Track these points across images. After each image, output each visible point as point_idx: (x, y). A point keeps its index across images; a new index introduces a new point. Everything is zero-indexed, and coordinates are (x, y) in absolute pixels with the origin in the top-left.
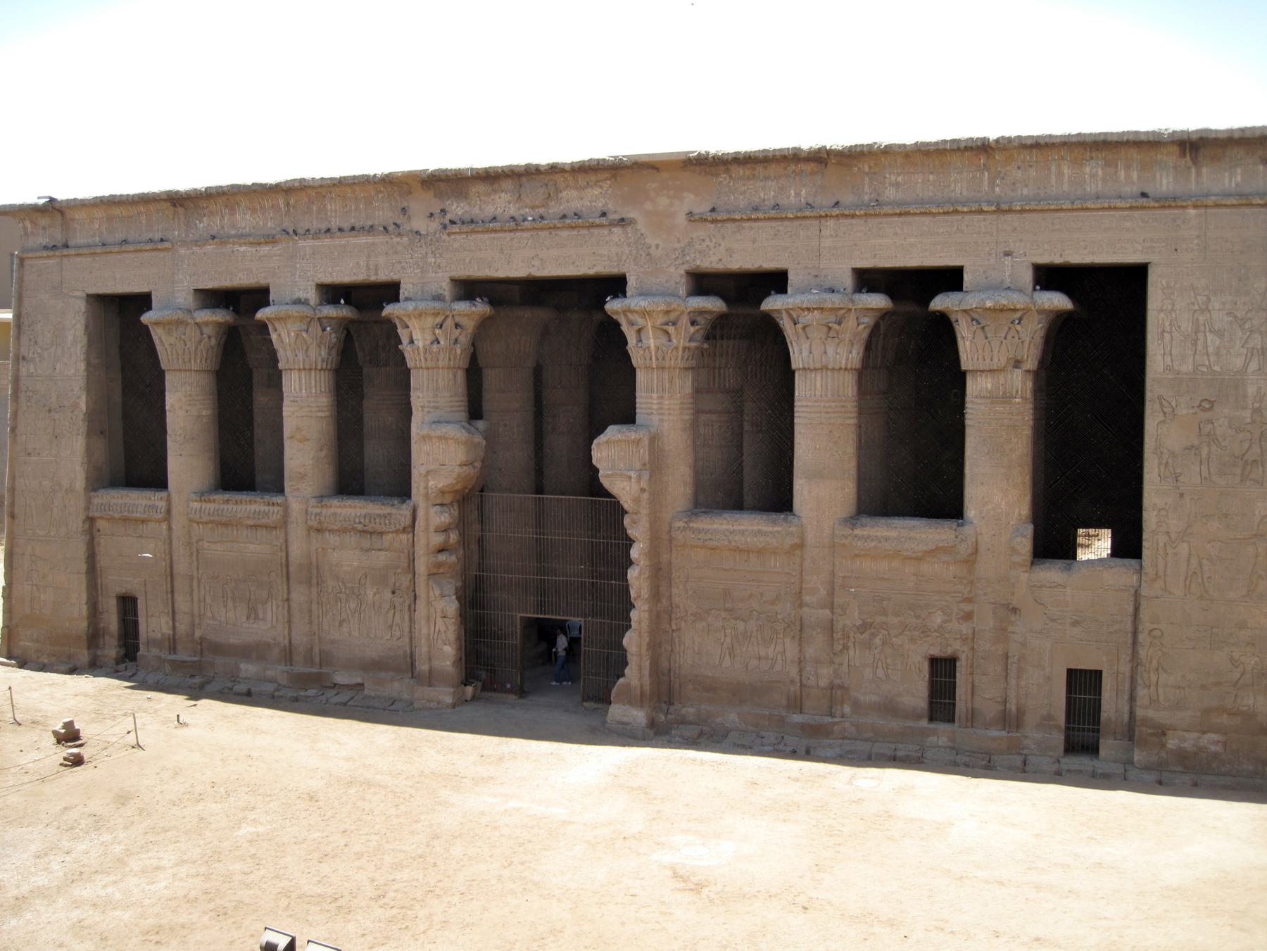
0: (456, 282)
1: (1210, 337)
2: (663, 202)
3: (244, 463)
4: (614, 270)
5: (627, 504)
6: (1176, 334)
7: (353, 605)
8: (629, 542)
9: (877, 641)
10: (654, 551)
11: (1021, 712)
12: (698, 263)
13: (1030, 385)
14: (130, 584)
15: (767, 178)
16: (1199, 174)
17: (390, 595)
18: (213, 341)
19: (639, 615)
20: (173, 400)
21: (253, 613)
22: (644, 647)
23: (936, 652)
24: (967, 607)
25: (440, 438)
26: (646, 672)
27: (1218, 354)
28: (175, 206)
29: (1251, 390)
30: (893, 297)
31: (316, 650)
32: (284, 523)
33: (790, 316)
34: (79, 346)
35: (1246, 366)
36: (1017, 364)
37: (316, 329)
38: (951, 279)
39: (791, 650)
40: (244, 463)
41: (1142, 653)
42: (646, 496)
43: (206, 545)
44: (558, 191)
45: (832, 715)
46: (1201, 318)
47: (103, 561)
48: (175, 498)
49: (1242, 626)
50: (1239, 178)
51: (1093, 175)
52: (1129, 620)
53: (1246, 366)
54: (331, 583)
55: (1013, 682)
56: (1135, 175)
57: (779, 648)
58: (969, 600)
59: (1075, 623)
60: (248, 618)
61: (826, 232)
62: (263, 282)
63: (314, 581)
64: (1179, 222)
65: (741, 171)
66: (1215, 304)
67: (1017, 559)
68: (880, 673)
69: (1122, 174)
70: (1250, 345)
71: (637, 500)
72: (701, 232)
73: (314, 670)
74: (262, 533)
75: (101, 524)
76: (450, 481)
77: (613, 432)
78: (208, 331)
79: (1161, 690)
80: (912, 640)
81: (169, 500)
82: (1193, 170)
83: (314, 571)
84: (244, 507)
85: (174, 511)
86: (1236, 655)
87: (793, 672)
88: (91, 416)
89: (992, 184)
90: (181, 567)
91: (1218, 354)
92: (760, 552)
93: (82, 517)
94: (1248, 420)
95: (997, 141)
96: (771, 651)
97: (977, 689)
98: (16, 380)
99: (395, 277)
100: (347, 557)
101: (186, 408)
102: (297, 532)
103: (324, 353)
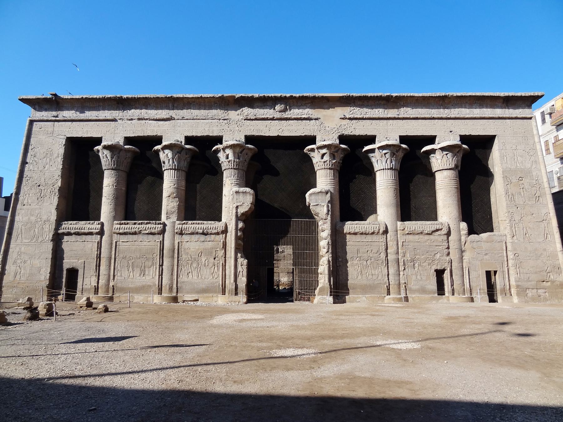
0: (246, 137)
9: (416, 265)
12: (343, 133)
21: (143, 273)
23: (439, 268)
25: (243, 192)
27: (522, 162)
28: (118, 103)
29: (534, 174)
32: (163, 232)
34: (60, 158)
43: (121, 243)
49: (545, 250)
59: (486, 254)
60: (140, 275)
61: (389, 124)
63: (176, 255)
66: (518, 147)
68: (419, 277)
73: (174, 295)
76: (247, 209)
78: (129, 155)
80: (429, 264)
83: (176, 252)
84: (143, 226)
86: (544, 261)
91: (522, 162)
96: (377, 271)
100: (192, 245)
103: (186, 163)
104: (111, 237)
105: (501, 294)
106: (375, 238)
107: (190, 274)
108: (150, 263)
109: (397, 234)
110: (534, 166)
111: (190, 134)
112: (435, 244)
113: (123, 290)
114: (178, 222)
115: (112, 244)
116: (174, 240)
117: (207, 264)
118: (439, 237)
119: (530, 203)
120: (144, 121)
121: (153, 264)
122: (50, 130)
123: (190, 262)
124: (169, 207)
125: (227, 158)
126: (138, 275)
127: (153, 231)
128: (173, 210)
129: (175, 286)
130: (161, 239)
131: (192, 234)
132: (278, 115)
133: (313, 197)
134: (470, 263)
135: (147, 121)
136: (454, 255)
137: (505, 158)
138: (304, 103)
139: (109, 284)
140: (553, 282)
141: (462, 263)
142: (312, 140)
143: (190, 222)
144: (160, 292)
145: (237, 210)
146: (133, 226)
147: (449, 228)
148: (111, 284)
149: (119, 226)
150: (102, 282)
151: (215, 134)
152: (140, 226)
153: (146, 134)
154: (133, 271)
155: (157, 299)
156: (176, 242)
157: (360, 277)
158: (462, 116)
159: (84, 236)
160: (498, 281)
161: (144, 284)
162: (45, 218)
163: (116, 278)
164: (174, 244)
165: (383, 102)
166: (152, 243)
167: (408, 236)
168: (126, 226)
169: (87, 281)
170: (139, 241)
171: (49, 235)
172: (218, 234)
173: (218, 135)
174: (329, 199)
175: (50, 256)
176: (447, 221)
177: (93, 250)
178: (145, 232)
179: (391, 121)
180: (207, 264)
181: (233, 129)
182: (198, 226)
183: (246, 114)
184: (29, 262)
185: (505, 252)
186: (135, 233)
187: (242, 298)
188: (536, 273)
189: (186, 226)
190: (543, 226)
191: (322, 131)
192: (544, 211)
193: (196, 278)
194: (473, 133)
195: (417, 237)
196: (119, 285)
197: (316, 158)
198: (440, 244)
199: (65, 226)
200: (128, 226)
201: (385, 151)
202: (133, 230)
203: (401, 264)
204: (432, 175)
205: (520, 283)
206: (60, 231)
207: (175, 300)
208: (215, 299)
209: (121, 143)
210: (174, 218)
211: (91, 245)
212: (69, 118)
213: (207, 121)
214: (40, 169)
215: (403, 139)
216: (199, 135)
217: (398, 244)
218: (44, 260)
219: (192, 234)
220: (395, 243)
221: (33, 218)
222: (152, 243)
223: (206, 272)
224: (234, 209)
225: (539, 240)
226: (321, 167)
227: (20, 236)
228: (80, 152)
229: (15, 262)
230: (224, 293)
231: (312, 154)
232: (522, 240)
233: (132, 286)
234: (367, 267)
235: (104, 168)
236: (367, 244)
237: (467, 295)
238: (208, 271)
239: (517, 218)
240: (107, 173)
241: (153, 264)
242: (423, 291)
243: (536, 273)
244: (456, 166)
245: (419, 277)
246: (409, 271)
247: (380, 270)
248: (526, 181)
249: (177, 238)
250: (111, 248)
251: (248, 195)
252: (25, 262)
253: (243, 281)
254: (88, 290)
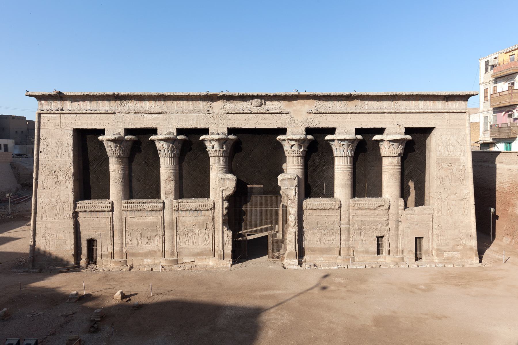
1: (451, 147)
9: (363, 233)
14: (92, 235)
21: (149, 241)
23: (379, 235)
25: (228, 179)
27: (453, 151)
29: (462, 161)
34: (70, 147)
49: (462, 222)
54: (181, 228)
59: (417, 224)
60: (147, 243)
62: (154, 127)
63: (175, 227)
66: (452, 138)
68: (364, 242)
72: (311, 116)
78: (129, 143)
80: (372, 232)
83: (175, 225)
84: (146, 204)
86: (461, 230)
91: (453, 151)
99: (207, 127)
100: (187, 219)
104: (121, 213)
105: (425, 254)
106: (332, 212)
107: (187, 242)
108: (155, 234)
109: (349, 209)
110: (462, 154)
111: (181, 127)
112: (379, 217)
113: (134, 255)
114: (175, 201)
115: (122, 219)
116: (172, 215)
117: (200, 234)
118: (381, 212)
119: (455, 185)
120: (140, 114)
122: (58, 122)
123: (186, 233)
124: (167, 189)
125: (213, 148)
126: (145, 243)
127: (155, 209)
128: (170, 191)
129: (175, 251)
130: (162, 215)
131: (187, 210)
132: (255, 110)
133: (283, 182)
134: (403, 231)
135: (143, 114)
136: (392, 225)
139: (122, 250)
140: (465, 246)
141: (398, 230)
142: (283, 131)
144: (164, 255)
146: (139, 205)
148: (125, 250)
149: (126, 205)
150: (117, 249)
151: (202, 126)
152: (144, 205)
153: (143, 127)
154: (141, 240)
155: (163, 262)
156: (174, 217)
157: (319, 242)
158: (408, 111)
159: (99, 213)
160: (425, 244)
161: (151, 250)
162: (64, 199)
163: (127, 246)
164: (173, 218)
165: (343, 99)
166: (155, 218)
167: (357, 211)
168: (133, 205)
169: (103, 248)
170: (142, 214)
172: (208, 210)
173: (205, 127)
174: (297, 183)
175: (73, 231)
176: (389, 198)
177: (107, 224)
178: (149, 209)
180: (200, 234)
181: (218, 122)
182: (191, 204)
183: (228, 108)
184: (55, 235)
185: (431, 222)
187: (229, 261)
188: (453, 239)
189: (182, 204)
191: (292, 124)
192: (465, 191)
193: (192, 244)
195: (364, 211)
196: (131, 251)
197: (286, 147)
198: (382, 216)
199: (82, 205)
200: (134, 204)
201: (342, 143)
202: (139, 209)
203: (351, 232)
204: (380, 159)
205: (440, 247)
207: (176, 262)
208: (207, 260)
209: (122, 134)
210: (172, 197)
211: (105, 220)
212: (73, 112)
213: (195, 115)
214: (54, 157)
216: (189, 127)
217: (349, 217)
218: (68, 234)
219: (187, 210)
220: (347, 216)
221: (53, 200)
222: (155, 218)
223: (199, 240)
224: (221, 192)
225: (459, 215)
226: (290, 155)
227: (45, 214)
228: (86, 141)
229: (43, 236)
230: (214, 256)
231: (283, 143)
233: (141, 252)
234: (325, 234)
235: (109, 155)
236: (325, 217)
237: (399, 256)
238: (201, 239)
239: (444, 197)
240: (111, 160)
241: (157, 235)
242: (367, 252)
243: (453, 239)
244: (400, 154)
245: (364, 242)
246: (356, 237)
249: (175, 214)
250: (122, 223)
251: (232, 181)
252: (52, 236)
253: (229, 248)
254: (106, 256)
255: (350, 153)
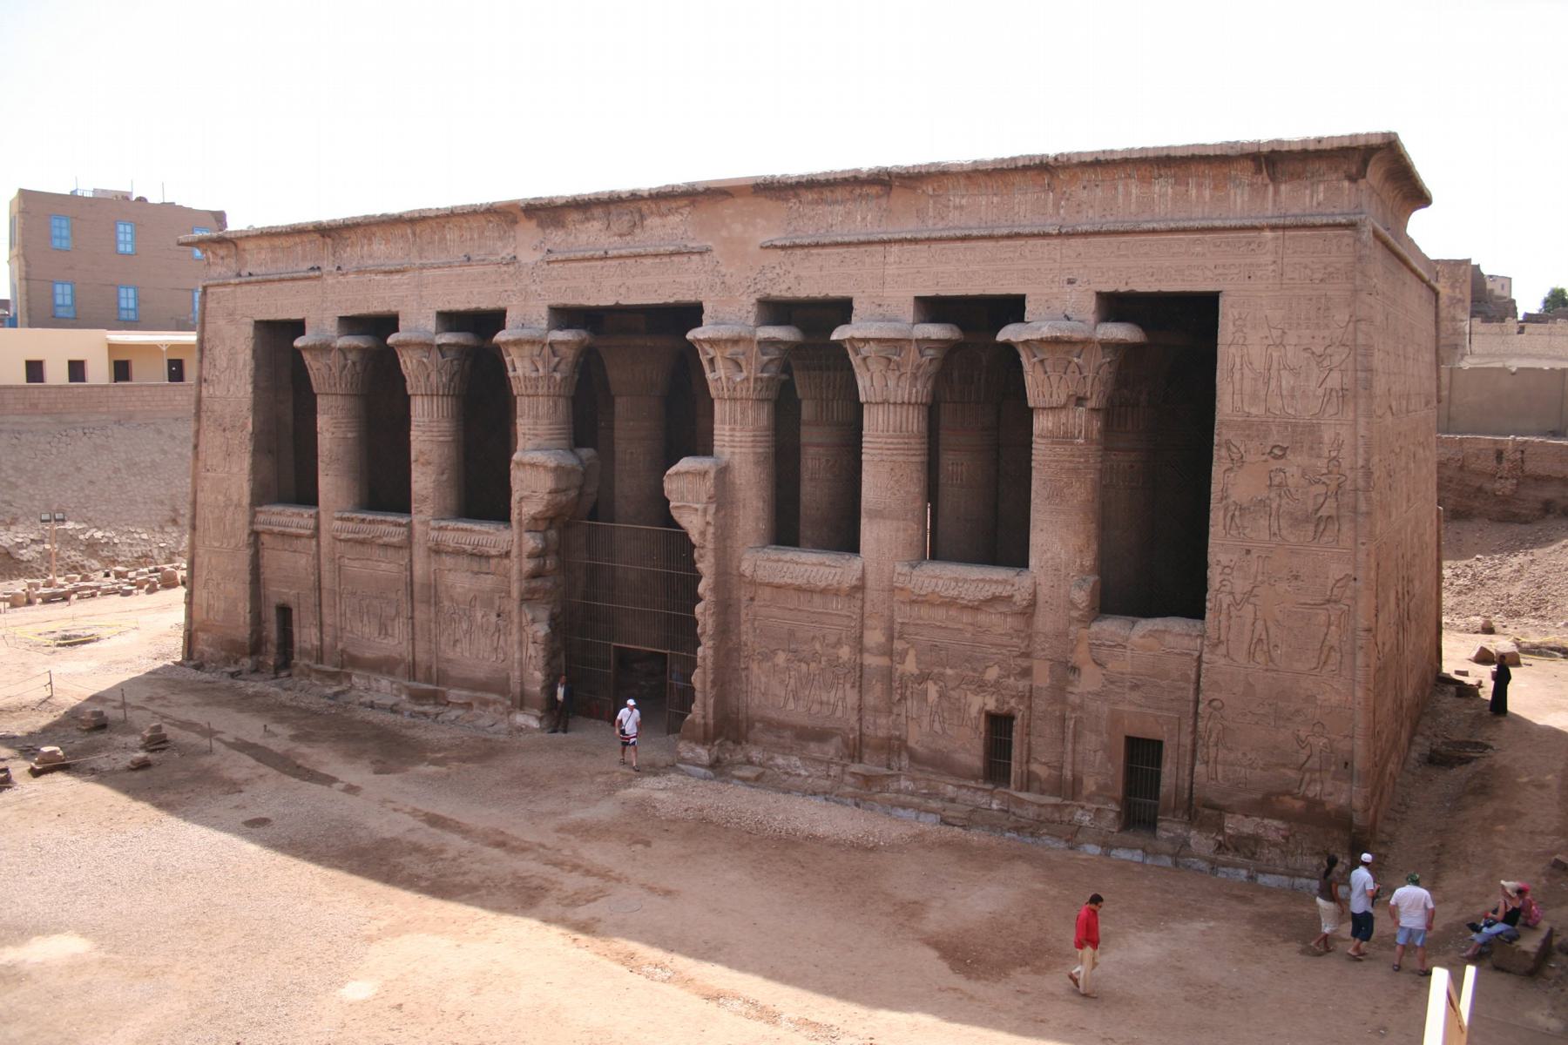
2: (738, 228)
3: (384, 487)
4: (687, 297)
5: (695, 537)
6: (1246, 371)
7: (465, 626)
8: (698, 578)
10: (717, 587)
11: (1077, 781)
13: (1097, 424)
14: (287, 594)
15: (836, 202)
16: (1276, 192)
17: (493, 618)
18: (358, 368)
19: (704, 651)
20: (323, 422)
21: (383, 629)
22: (709, 685)
23: (991, 705)
24: (1025, 663)
26: (710, 711)
30: (963, 328)
31: (434, 669)
32: (408, 543)
33: (853, 347)
35: (1323, 410)
36: (1080, 401)
37: (436, 354)
38: (1013, 308)
39: (852, 697)
40: (384, 487)
41: (1201, 724)
42: (711, 530)
44: (642, 218)
45: (889, 767)
46: (1275, 355)
47: (267, 573)
48: (323, 516)
50: (1321, 196)
51: (1163, 197)
52: (1192, 687)
53: (1323, 410)
54: (446, 603)
55: (1069, 747)
56: (1207, 193)
57: (840, 693)
58: (1026, 655)
59: (1135, 687)
61: (891, 259)
64: (1254, 246)
65: (810, 196)
66: (1292, 338)
67: (1075, 614)
68: (937, 726)
69: (1193, 192)
70: (1329, 384)
71: (703, 534)
73: (431, 687)
74: (390, 552)
75: (265, 538)
76: (540, 508)
77: (686, 464)
79: (1220, 768)
81: (317, 517)
82: (1271, 188)
85: (323, 528)
86: (1302, 734)
87: (854, 719)
88: (257, 436)
89: (1057, 206)
90: (327, 582)
92: (824, 592)
93: (247, 531)
94: (1324, 471)
95: (1056, 159)
97: (1036, 752)
98: (199, 401)
99: (501, 304)
101: (332, 430)
102: (419, 553)
108: (393, 612)
110: (1331, 410)
114: (433, 523)
121: (398, 614)
137: (1237, 376)
138: (674, 205)
143: (452, 524)
145: (520, 509)
147: (1035, 594)
157: (791, 705)
162: (235, 498)
166: (393, 567)
171: (243, 536)
175: (248, 578)
179: (895, 248)
186: (362, 542)
190: (1322, 618)
194: (1141, 287)
195: (941, 613)
206: (259, 528)
215: (932, 308)
225: (1298, 666)
232: (1241, 658)
247: (840, 693)
248: (1294, 465)
255: (919, 391)
